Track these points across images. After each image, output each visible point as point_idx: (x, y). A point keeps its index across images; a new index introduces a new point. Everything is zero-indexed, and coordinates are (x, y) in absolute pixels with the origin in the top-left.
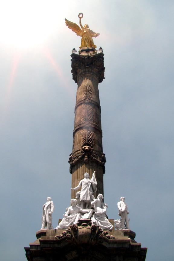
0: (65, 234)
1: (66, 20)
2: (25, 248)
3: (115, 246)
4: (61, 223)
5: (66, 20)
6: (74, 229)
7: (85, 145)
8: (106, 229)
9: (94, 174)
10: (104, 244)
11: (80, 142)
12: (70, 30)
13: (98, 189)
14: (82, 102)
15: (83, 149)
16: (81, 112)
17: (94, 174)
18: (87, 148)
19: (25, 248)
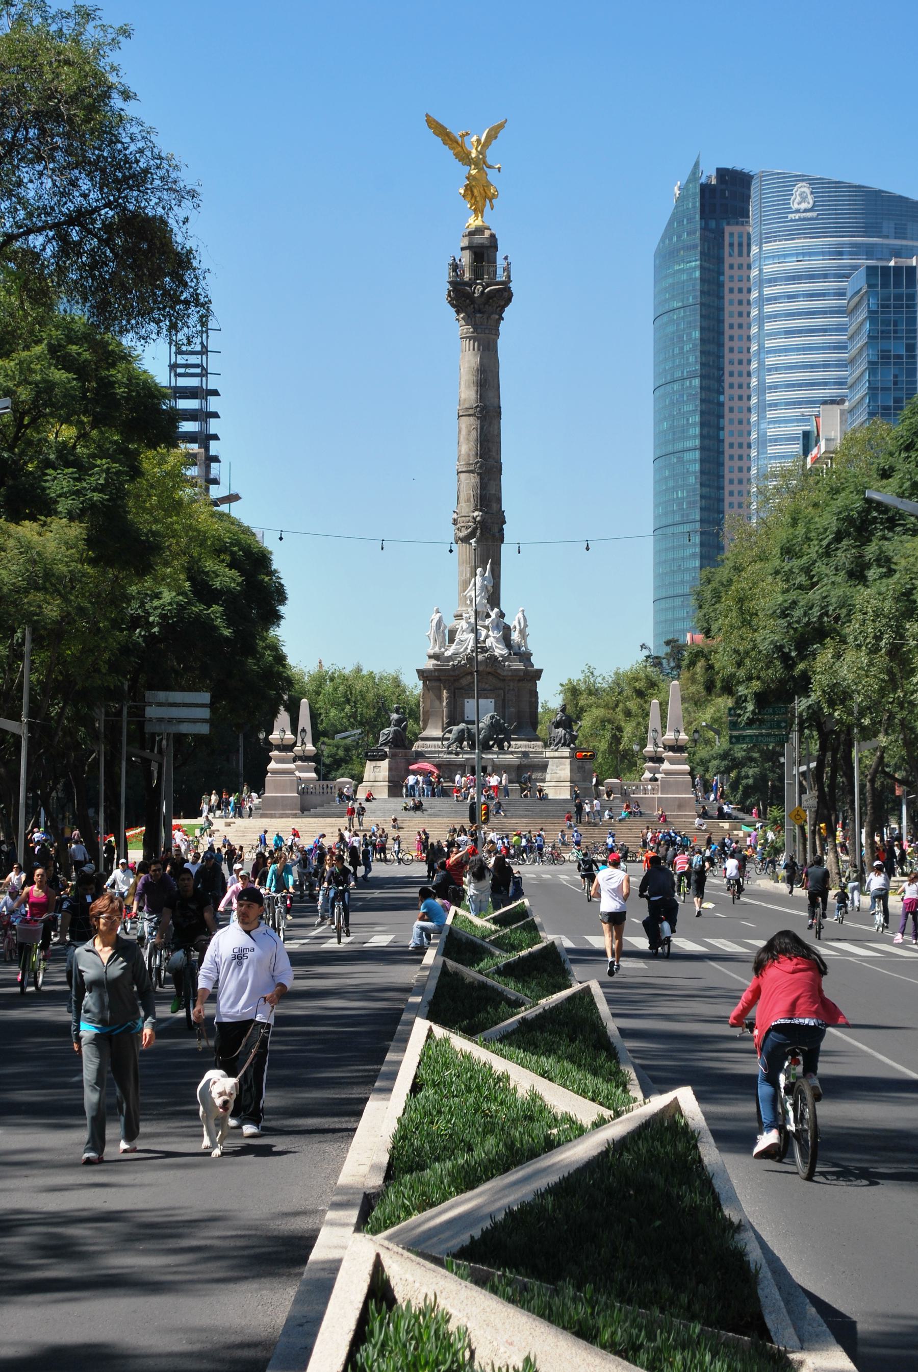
0: (460, 662)
1: (427, 115)
2: (418, 671)
3: (510, 674)
4: (454, 646)
5: (427, 115)
6: (470, 659)
7: (476, 510)
8: (502, 656)
9: (488, 566)
10: (499, 671)
11: (468, 500)
12: (439, 140)
13: (494, 598)
14: (471, 412)
15: (474, 518)
16: (469, 432)
17: (488, 566)
18: (478, 519)
19: (418, 671)
